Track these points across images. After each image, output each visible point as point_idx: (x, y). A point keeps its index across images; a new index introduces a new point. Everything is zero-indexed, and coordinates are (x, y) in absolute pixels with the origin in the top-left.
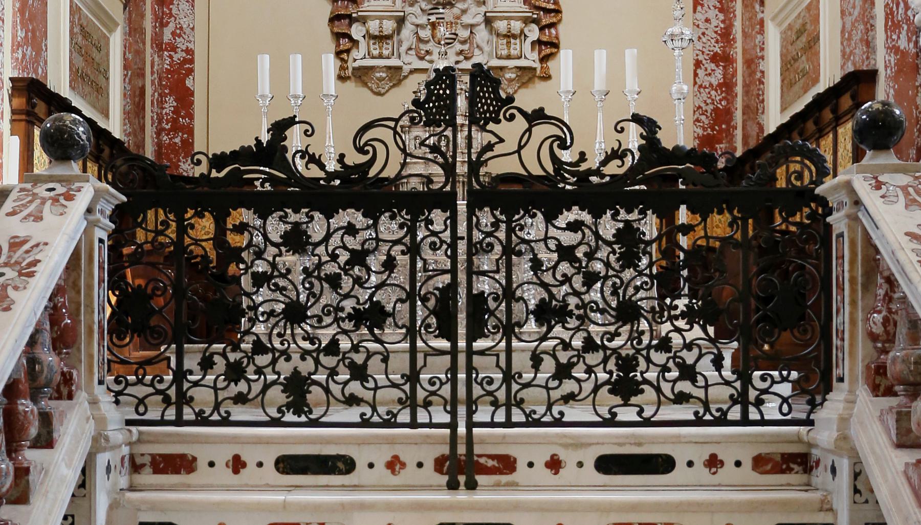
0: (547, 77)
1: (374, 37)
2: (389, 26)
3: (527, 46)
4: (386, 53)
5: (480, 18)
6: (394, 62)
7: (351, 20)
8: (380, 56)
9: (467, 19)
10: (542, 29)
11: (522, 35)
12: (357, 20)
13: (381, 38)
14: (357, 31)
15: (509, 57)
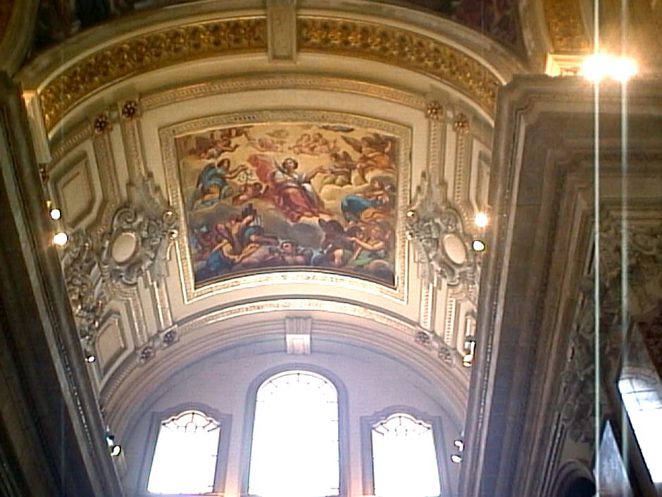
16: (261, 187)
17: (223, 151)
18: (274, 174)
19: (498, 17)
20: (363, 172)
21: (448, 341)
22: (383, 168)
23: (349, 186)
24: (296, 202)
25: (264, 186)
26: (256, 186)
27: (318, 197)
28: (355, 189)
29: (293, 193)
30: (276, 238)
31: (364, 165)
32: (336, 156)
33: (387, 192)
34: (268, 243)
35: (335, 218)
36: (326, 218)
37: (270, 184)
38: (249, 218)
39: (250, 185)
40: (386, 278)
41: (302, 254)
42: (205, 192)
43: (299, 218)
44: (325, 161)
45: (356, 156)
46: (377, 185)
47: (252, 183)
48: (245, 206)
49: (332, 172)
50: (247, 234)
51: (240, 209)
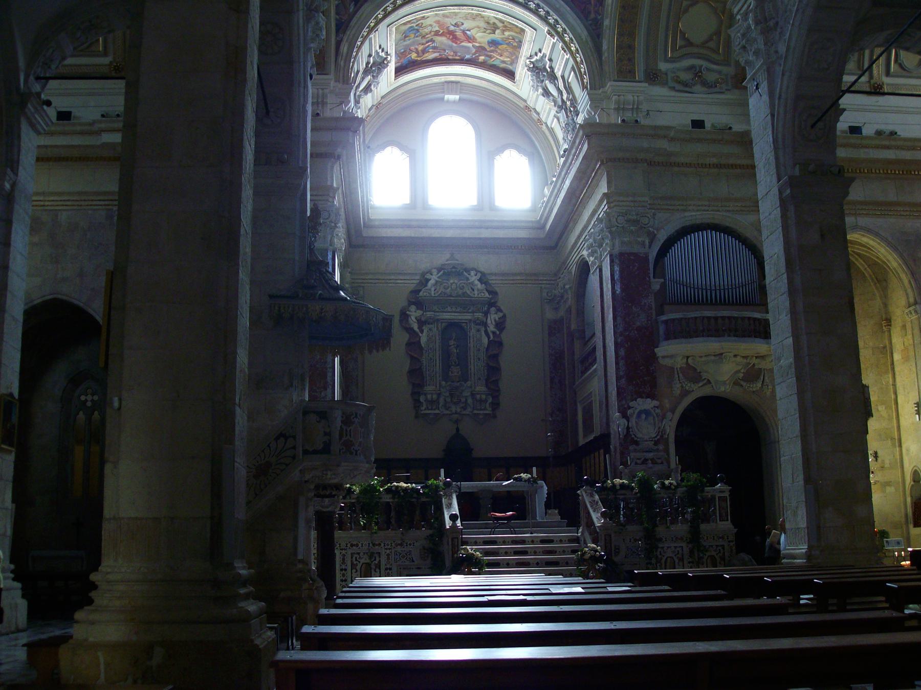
0: (495, 417)
2: (435, 397)
3: (488, 405)
6: (437, 411)
7: (419, 394)
10: (493, 398)
11: (486, 401)
13: (432, 402)
14: (422, 399)
15: (481, 410)
19: (592, 16)
20: (503, 31)
28: (498, 36)
32: (488, 23)
36: (477, 45)
40: (510, 74)
42: (406, 37)
44: (482, 24)
51: (424, 41)
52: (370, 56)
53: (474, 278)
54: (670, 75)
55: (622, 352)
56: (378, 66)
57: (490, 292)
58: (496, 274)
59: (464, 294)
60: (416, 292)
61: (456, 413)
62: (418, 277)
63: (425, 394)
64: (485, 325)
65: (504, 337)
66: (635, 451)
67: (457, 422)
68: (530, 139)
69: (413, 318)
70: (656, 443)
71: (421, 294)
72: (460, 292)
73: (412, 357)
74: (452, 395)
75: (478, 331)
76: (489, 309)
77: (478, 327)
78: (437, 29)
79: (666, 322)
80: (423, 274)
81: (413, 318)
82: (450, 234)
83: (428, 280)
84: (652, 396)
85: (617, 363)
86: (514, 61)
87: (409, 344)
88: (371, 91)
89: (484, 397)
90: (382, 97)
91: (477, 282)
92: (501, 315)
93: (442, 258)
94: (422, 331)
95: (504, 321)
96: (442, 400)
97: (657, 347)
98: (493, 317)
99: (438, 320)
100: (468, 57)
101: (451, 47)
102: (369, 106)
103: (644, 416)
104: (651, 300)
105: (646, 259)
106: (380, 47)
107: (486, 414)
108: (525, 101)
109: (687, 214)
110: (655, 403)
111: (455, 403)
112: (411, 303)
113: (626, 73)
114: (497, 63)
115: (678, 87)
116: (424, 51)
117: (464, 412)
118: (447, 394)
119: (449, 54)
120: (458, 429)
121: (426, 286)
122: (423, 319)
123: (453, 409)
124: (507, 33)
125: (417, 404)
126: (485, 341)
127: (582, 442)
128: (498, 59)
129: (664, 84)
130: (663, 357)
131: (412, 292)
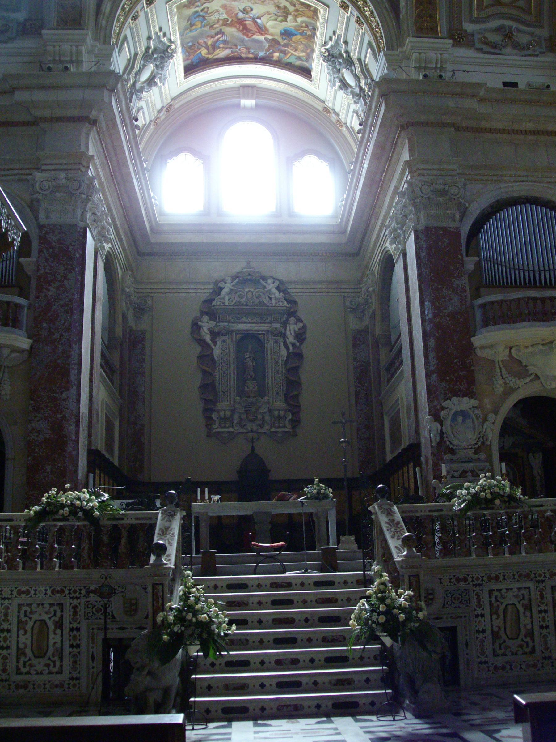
0: (295, 435)
1: (223, 419)
2: (228, 413)
3: (287, 422)
4: (227, 425)
5: (266, 410)
6: (231, 430)
7: (212, 411)
8: (225, 427)
9: (261, 411)
10: (293, 414)
11: (285, 417)
12: (215, 411)
13: (225, 419)
14: (214, 416)
15: (279, 427)
16: (228, 20)
17: (205, 3)
18: (237, 14)
20: (296, 17)
21: (343, 118)
22: (309, 17)
23: (286, 23)
24: (251, 28)
25: (230, 20)
26: (225, 20)
27: (265, 27)
28: (290, 24)
29: (250, 24)
30: (236, 45)
31: (296, 13)
32: (279, 7)
33: (311, 31)
34: (231, 48)
35: (276, 37)
36: (270, 37)
37: (234, 19)
38: (219, 36)
39: (221, 20)
40: (306, 72)
41: (252, 53)
42: (191, 25)
43: (252, 36)
44: (272, 9)
45: (291, 8)
46: (304, 25)
47: (223, 18)
48: (218, 30)
49: (275, 15)
50: (217, 44)
51: (213, 32)
52: (149, 38)
53: (271, 286)
54: (477, 37)
55: (432, 343)
56: (160, 54)
57: (288, 301)
58: (294, 282)
59: (261, 303)
60: (209, 301)
61: (252, 431)
62: (211, 286)
63: (218, 411)
64: (284, 336)
65: (305, 349)
66: (452, 461)
67: (252, 441)
68: (333, 148)
69: (205, 329)
70: (476, 452)
71: (214, 303)
72: (257, 301)
73: (204, 372)
74: (247, 412)
75: (276, 342)
76: (287, 320)
77: (276, 338)
78: (225, 16)
79: (483, 306)
80: (216, 283)
81: (205, 329)
82: (245, 239)
83: (221, 289)
84: (470, 394)
85: (426, 356)
86: (309, 57)
87: (201, 357)
88: (156, 84)
89: (282, 413)
90: (173, 99)
91: (274, 291)
92: (300, 325)
93: (238, 266)
94: (215, 343)
95: (304, 333)
96: (236, 417)
97: (474, 336)
98: (292, 328)
99: (232, 331)
100: (262, 54)
101: (243, 41)
102: (159, 107)
103: (460, 419)
104: (464, 281)
105: (457, 234)
106: (161, 29)
107: (285, 432)
108: (323, 102)
109: (502, 185)
110: (474, 402)
111: (251, 421)
112: (203, 313)
113: (426, 27)
114: (292, 60)
115: (486, 48)
116: (215, 47)
117: (261, 431)
118: (242, 411)
119: (241, 50)
120: (253, 448)
121: (219, 294)
122: (216, 330)
123: (249, 426)
124: (299, 20)
125: (209, 421)
126: (284, 353)
127: (389, 457)
128: (294, 55)
129: (470, 45)
130: (482, 348)
131: (205, 301)
